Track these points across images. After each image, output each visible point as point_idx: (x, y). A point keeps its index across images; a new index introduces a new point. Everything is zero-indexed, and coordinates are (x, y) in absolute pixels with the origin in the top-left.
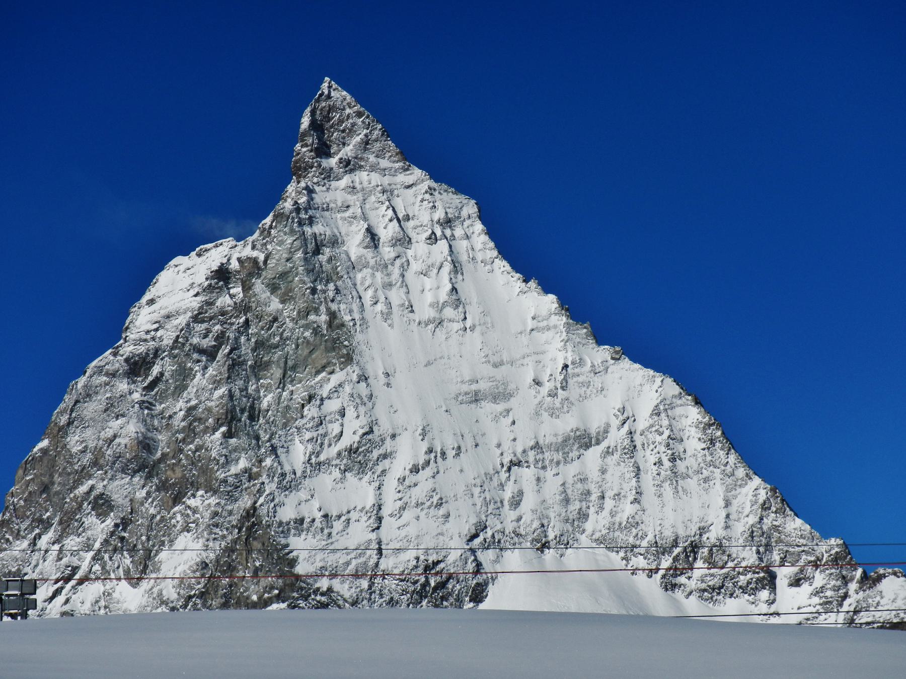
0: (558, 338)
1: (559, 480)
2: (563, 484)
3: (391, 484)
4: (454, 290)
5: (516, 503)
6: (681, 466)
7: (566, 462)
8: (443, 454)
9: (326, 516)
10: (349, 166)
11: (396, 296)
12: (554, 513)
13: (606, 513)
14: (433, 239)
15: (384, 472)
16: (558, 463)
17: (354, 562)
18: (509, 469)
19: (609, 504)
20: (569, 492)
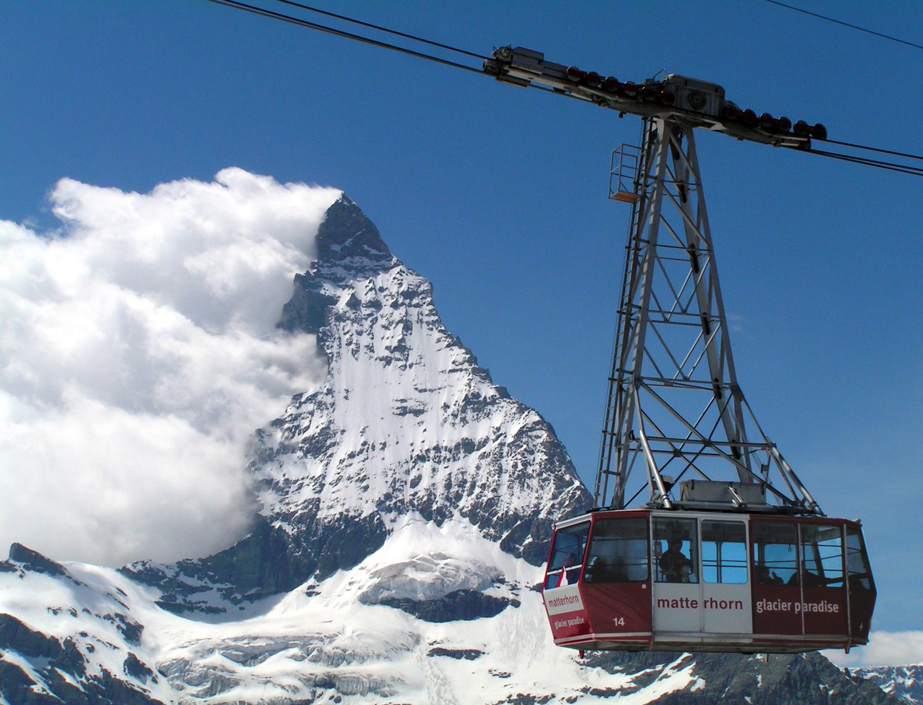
0: (466, 377)
1: (448, 471)
2: (450, 474)
3: (335, 462)
5: (415, 483)
6: (530, 470)
7: (454, 460)
9: (287, 480)
10: (350, 252)
11: (365, 340)
12: (440, 490)
13: (473, 496)
15: (331, 455)
16: (449, 460)
17: (300, 512)
18: (415, 462)
19: (477, 490)
20: (453, 479)
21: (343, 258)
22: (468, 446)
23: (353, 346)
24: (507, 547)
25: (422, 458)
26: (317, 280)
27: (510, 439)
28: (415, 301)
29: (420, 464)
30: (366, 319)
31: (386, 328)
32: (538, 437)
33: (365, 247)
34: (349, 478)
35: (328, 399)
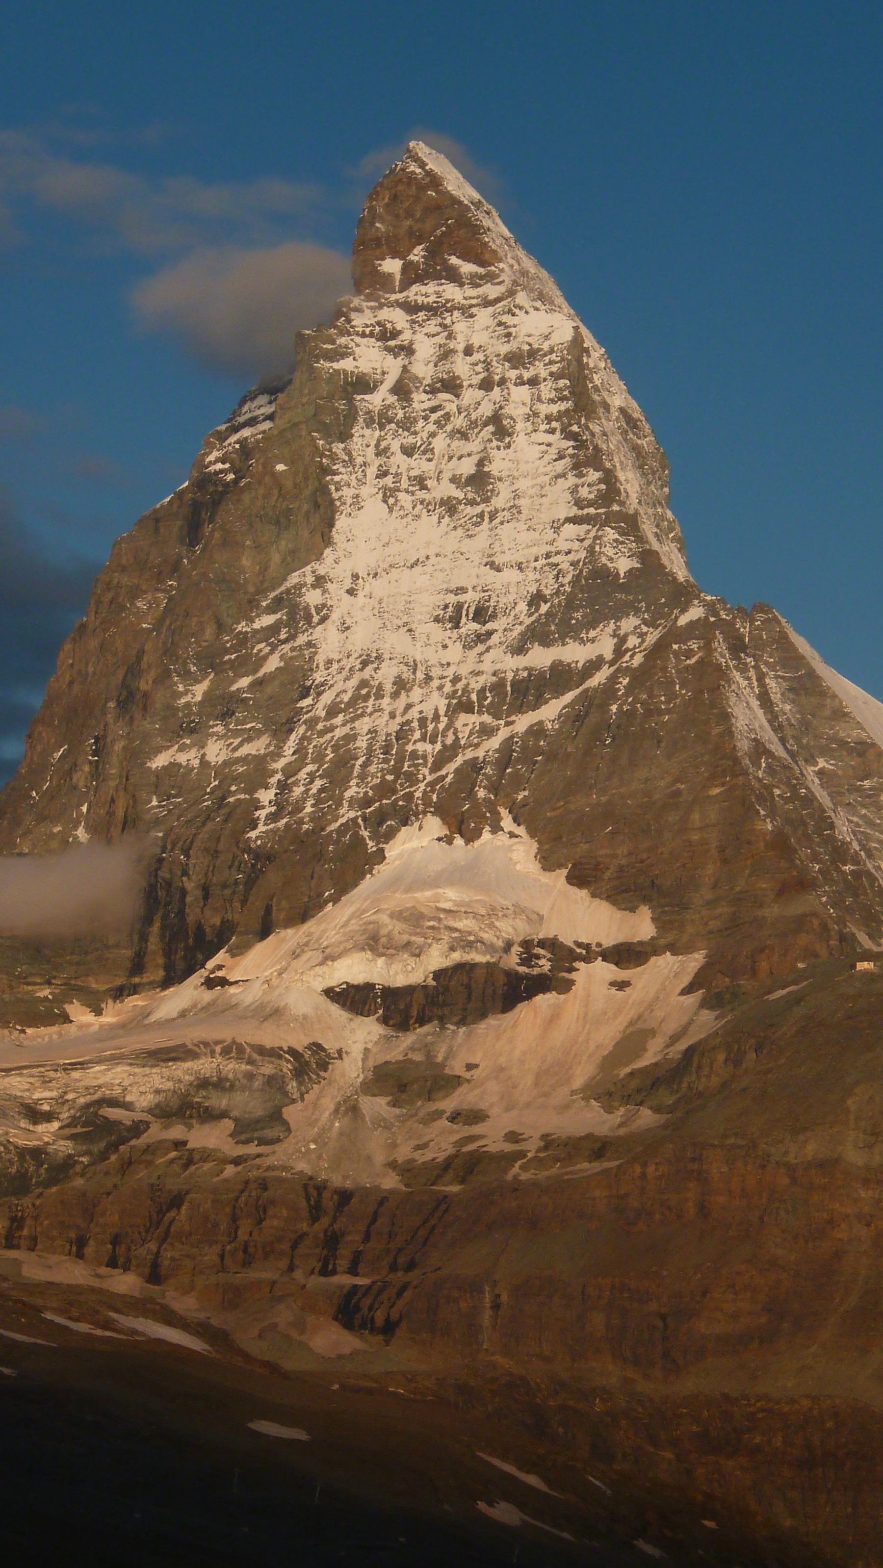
5: (440, 762)
8: (380, 687)
21: (406, 285)
22: (560, 677)
23: (389, 480)
24: (577, 879)
25: (468, 708)
26: (343, 340)
27: (638, 660)
28: (527, 375)
29: (463, 718)
30: (426, 418)
31: (464, 435)
32: (689, 654)
33: (454, 260)
34: (319, 758)
35: (313, 598)
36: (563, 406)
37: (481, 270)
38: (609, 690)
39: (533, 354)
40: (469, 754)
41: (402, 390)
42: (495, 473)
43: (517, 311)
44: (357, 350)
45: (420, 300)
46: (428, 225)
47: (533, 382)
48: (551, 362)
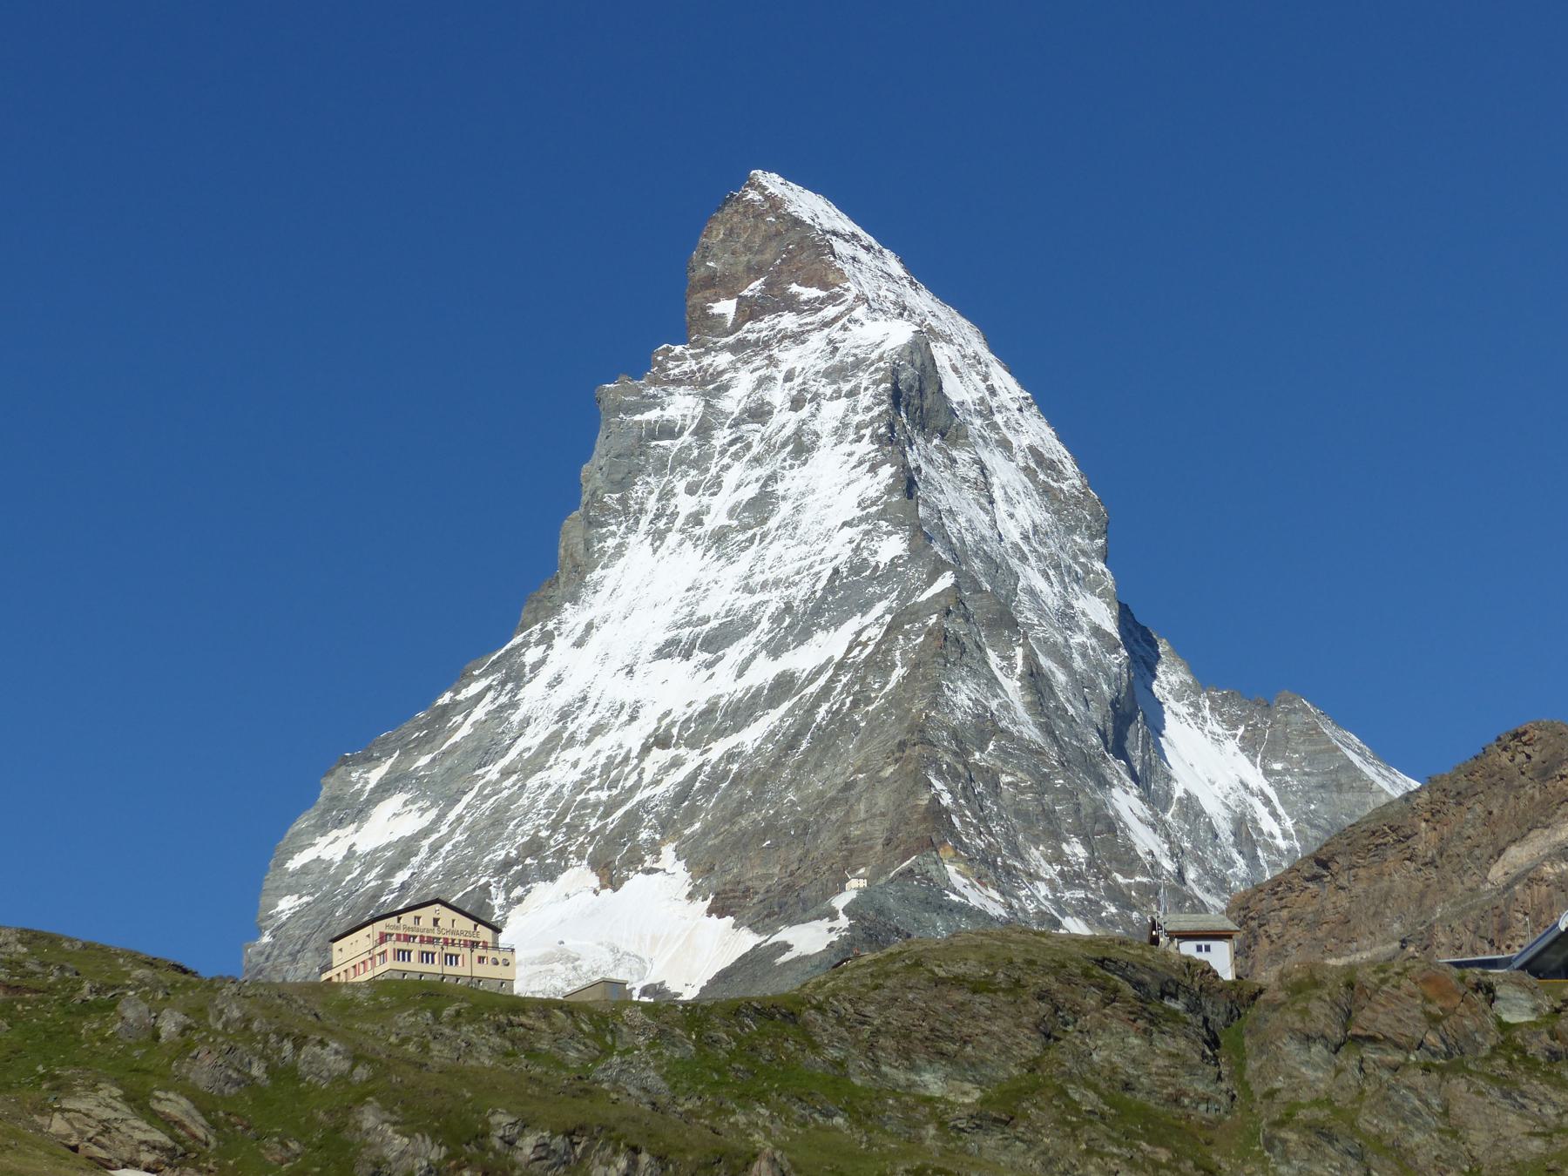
4: (773, 478)
10: (750, 311)
14: (796, 404)
21: (737, 326)
23: (661, 525)
28: (846, 387)
29: (656, 752)
33: (794, 288)
36: (876, 411)
37: (823, 294)
38: (826, 692)
39: (858, 364)
40: (647, 793)
41: (704, 431)
42: (780, 493)
43: (850, 326)
44: (667, 400)
45: (752, 337)
46: (768, 256)
47: (852, 394)
48: (877, 370)
